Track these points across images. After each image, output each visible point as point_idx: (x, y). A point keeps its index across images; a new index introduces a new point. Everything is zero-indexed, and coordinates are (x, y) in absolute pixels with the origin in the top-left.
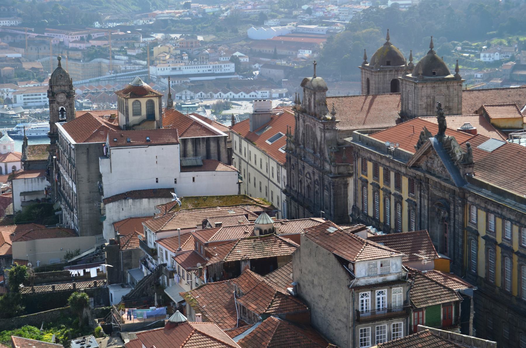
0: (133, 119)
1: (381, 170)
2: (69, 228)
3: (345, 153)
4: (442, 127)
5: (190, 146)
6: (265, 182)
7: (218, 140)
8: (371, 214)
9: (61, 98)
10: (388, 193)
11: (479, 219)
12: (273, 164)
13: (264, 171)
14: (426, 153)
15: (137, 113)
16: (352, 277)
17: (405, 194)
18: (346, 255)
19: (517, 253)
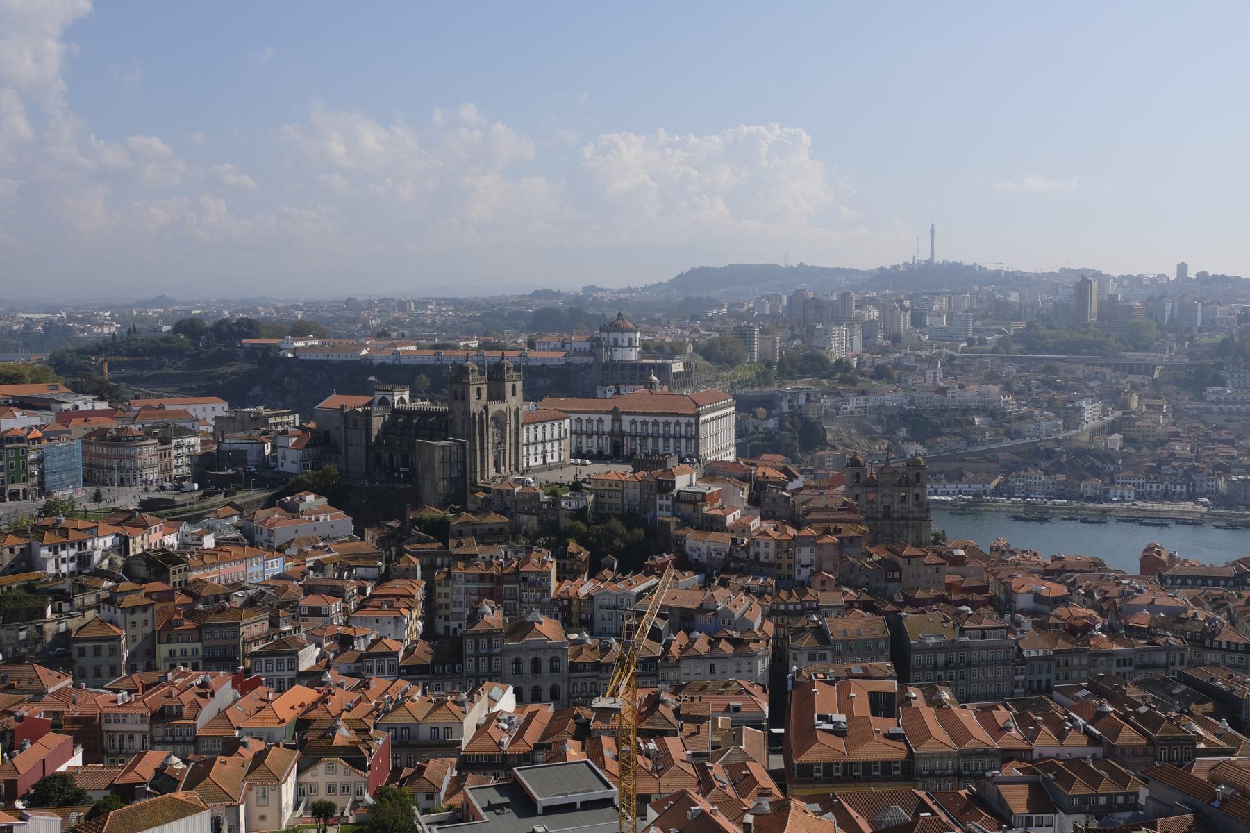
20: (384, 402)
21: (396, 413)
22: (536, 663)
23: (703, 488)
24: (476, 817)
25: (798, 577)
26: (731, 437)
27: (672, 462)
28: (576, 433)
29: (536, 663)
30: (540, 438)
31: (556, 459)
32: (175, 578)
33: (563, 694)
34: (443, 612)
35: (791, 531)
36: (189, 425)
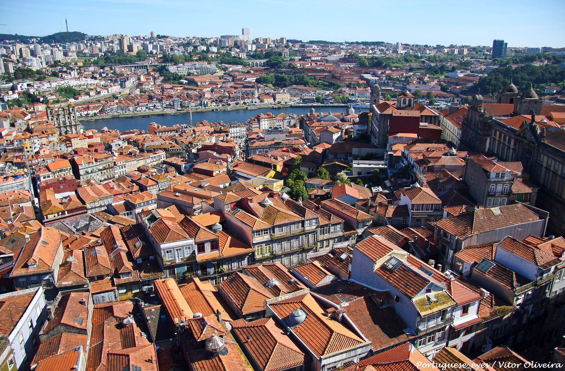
0: (402, 105)
1: (503, 135)
2: (374, 144)
3: (488, 126)
4: (533, 120)
5: (424, 119)
6: (452, 135)
7: (436, 117)
8: (495, 152)
9: (375, 95)
10: (504, 145)
11: (544, 160)
12: (456, 128)
13: (452, 131)
14: (524, 130)
15: (404, 103)
16: (488, 177)
17: (512, 146)
18: (488, 169)
19: (560, 176)
35: (29, 135)
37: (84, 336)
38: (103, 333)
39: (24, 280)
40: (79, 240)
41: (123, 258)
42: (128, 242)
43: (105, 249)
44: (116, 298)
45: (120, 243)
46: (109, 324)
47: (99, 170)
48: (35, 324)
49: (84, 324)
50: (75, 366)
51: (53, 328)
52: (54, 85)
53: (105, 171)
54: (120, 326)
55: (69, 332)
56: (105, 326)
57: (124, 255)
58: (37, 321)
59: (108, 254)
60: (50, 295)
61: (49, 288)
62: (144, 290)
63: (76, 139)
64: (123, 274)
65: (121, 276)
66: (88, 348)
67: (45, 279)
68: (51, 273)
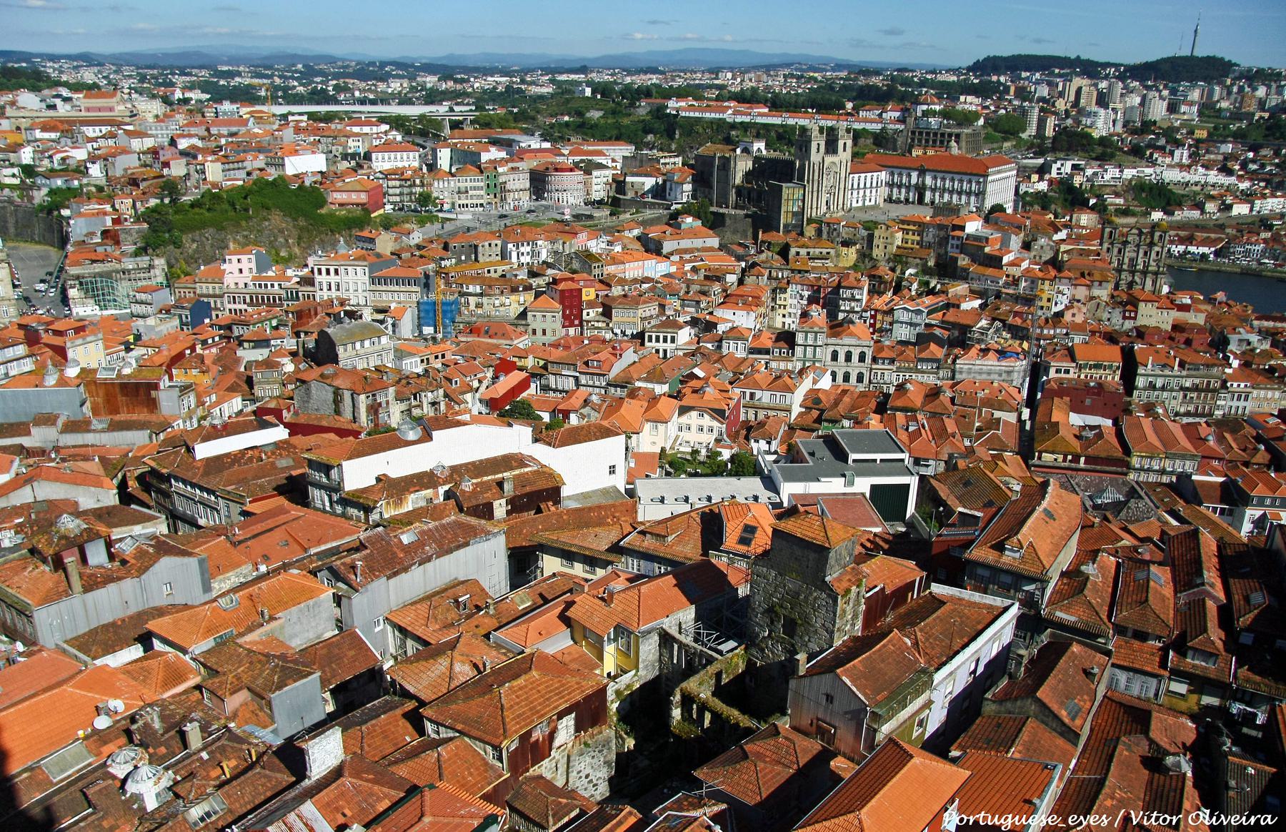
20: (746, 151)
21: (757, 160)
22: (848, 357)
23: (986, 232)
24: (803, 460)
25: (1055, 309)
26: (1011, 195)
27: (963, 212)
28: (891, 185)
29: (848, 357)
30: (862, 185)
31: (873, 203)
32: (596, 272)
33: (866, 380)
34: (782, 311)
35: (1053, 273)
36: (604, 162)
37: (1068, 746)
38: (1110, 761)
39: (987, 573)
40: (1096, 529)
41: (1209, 616)
42: (1231, 581)
43: (1169, 576)
44: (1156, 695)
45: (1211, 575)
46: (1129, 748)
47: (1182, 389)
48: (980, 669)
49: (1078, 722)
50: (1036, 801)
51: (1016, 699)
52: (1129, 173)
53: (1194, 395)
54: (1154, 762)
55: (1043, 722)
56: (1120, 747)
57: (1211, 605)
58: (986, 666)
59: (1176, 592)
60: (1029, 624)
61: (1025, 610)
62: (1235, 712)
63: (1150, 305)
64: (1195, 650)
65: (1190, 653)
66: (1068, 773)
67: (1026, 588)
68: (1042, 581)
